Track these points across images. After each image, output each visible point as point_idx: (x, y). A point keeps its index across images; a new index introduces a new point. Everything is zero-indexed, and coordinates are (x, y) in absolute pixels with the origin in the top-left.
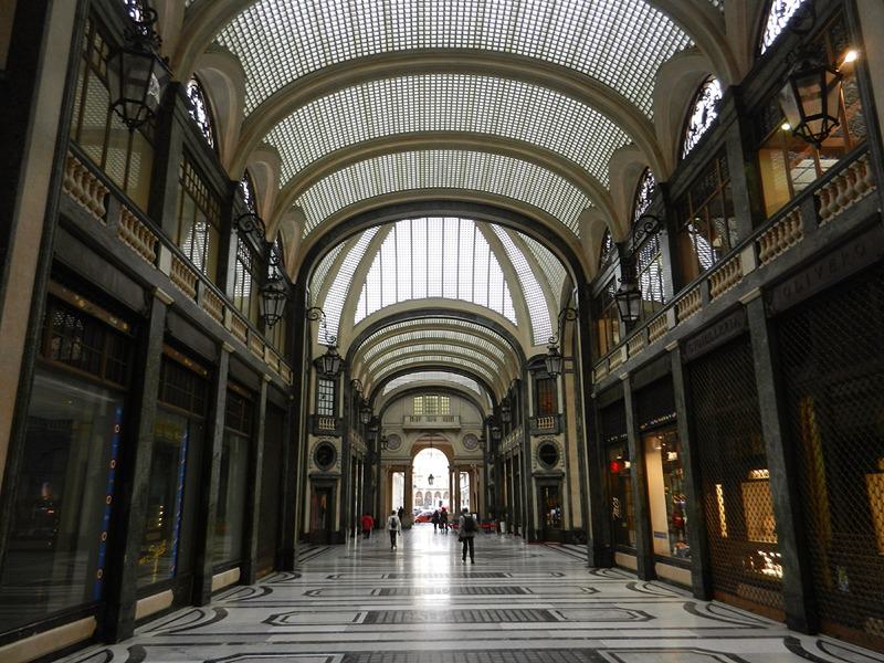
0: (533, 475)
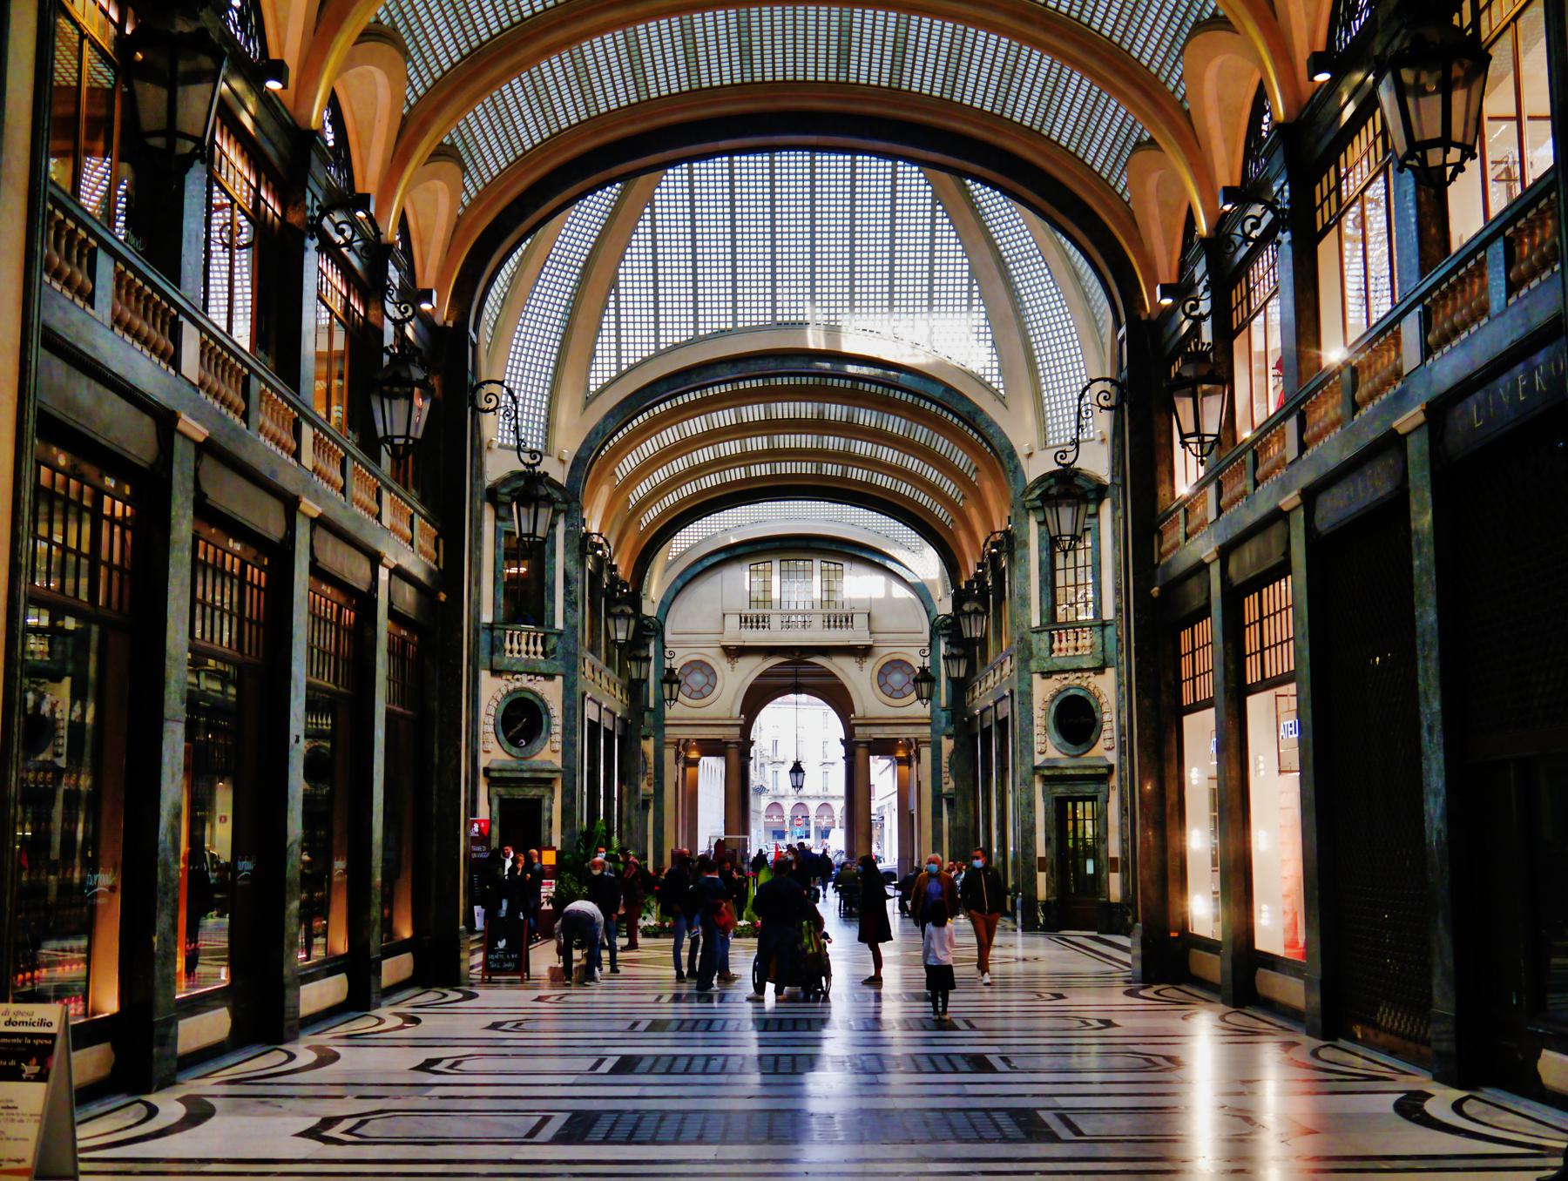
0: (1036, 769)
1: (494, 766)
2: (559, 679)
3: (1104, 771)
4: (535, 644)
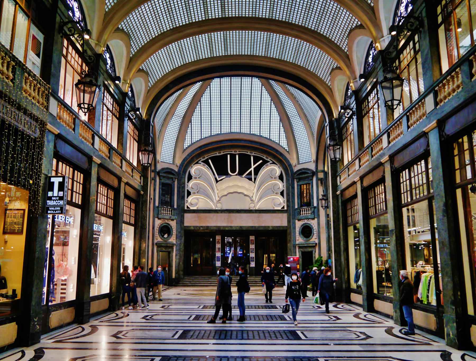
1: (159, 243)
2: (175, 221)
3: (314, 245)
4: (169, 212)
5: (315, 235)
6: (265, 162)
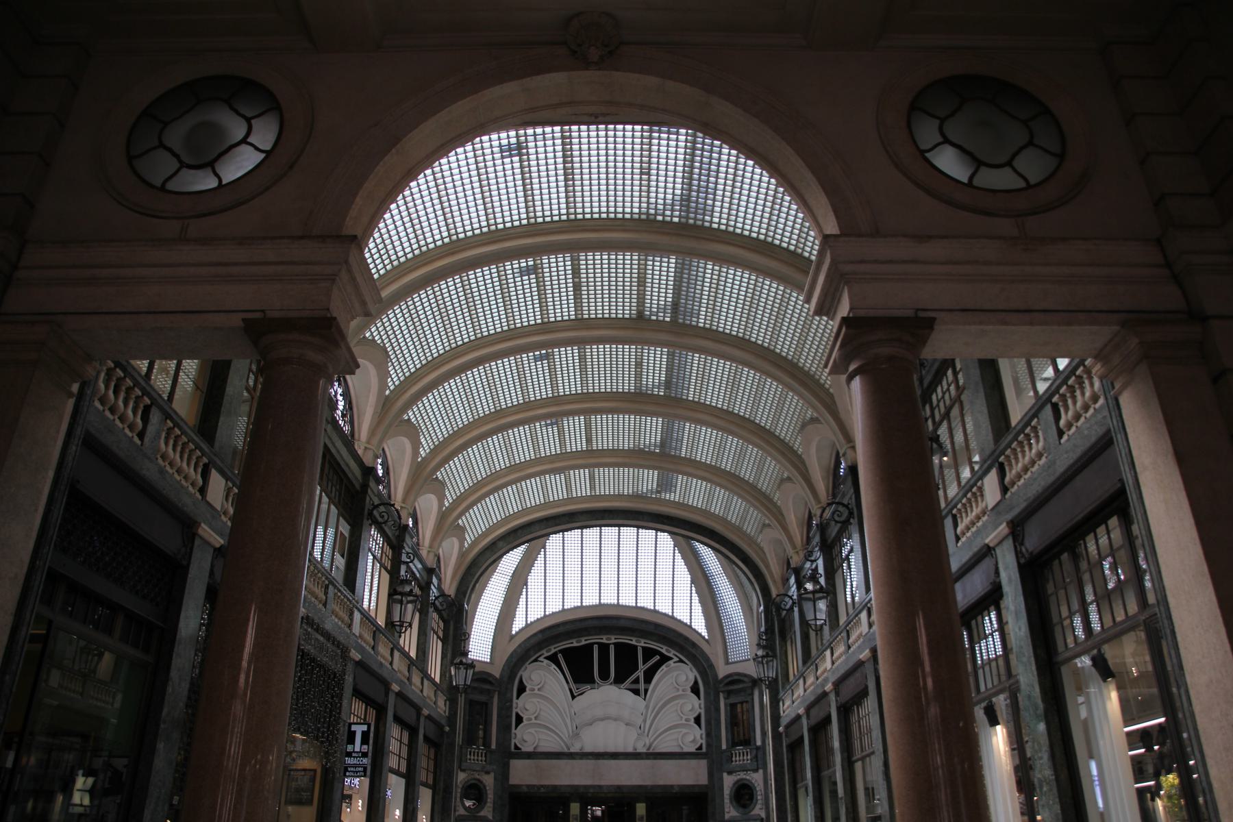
2: (492, 775)
5: (759, 802)
6: (665, 659)
